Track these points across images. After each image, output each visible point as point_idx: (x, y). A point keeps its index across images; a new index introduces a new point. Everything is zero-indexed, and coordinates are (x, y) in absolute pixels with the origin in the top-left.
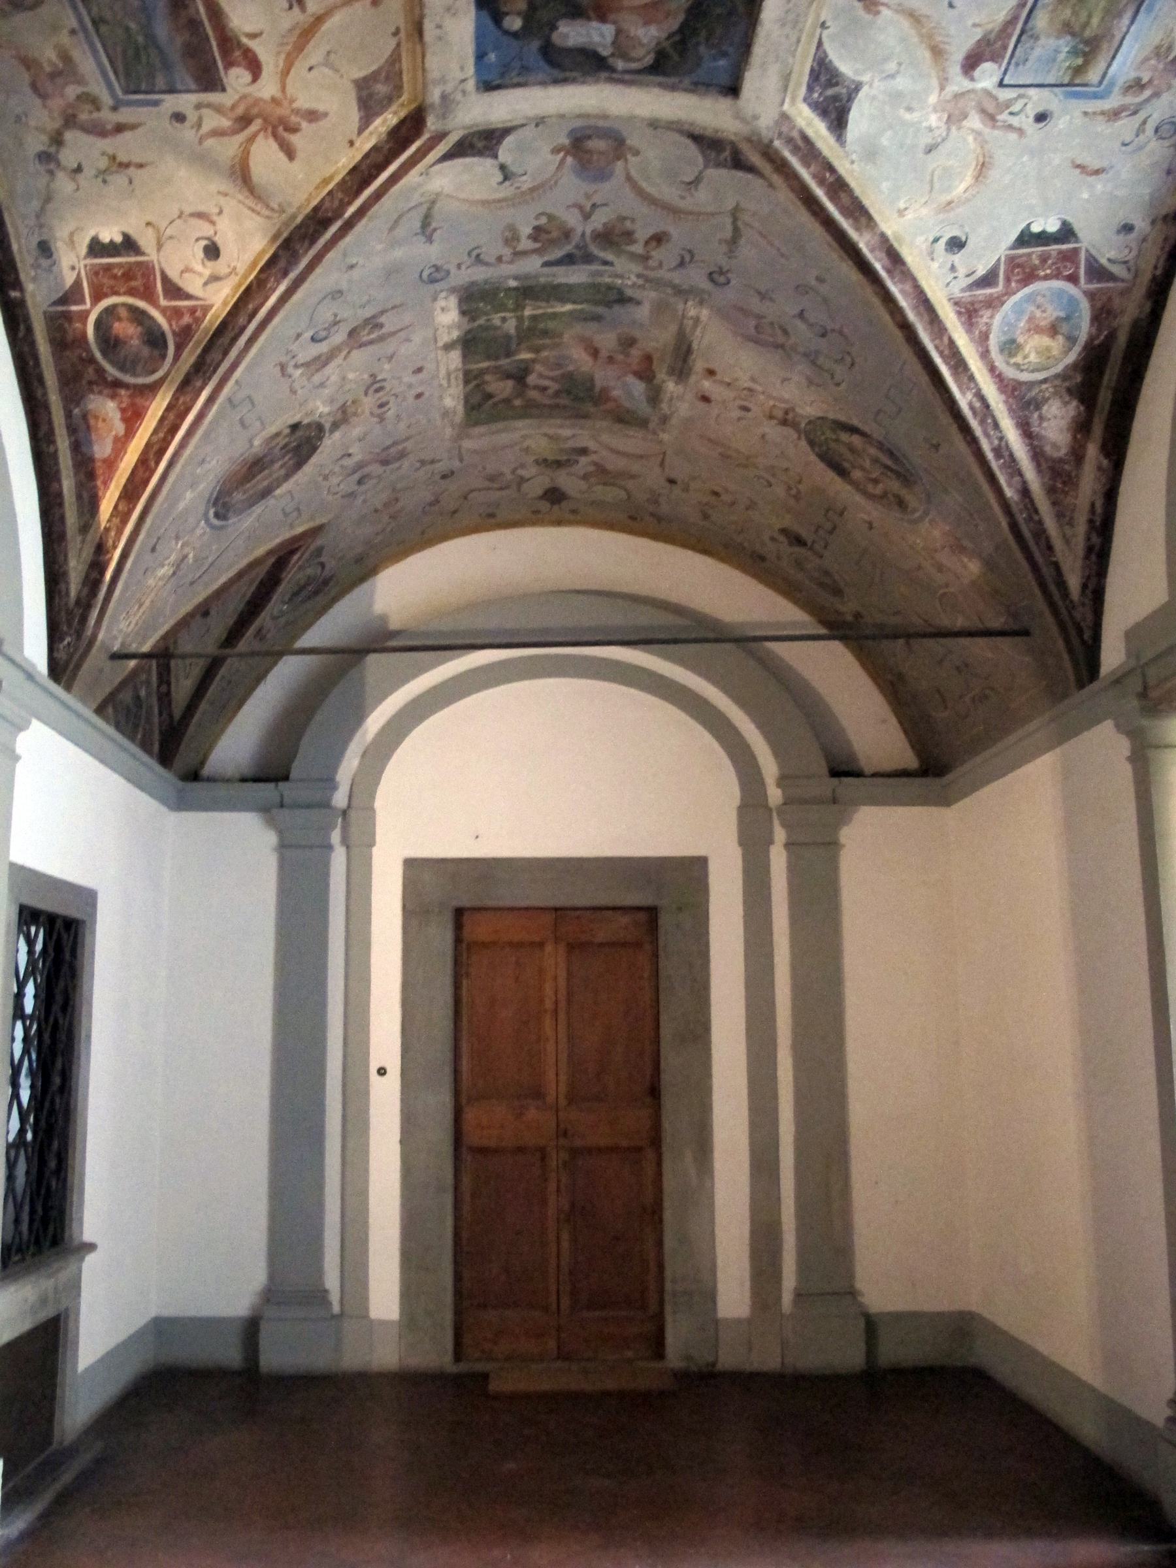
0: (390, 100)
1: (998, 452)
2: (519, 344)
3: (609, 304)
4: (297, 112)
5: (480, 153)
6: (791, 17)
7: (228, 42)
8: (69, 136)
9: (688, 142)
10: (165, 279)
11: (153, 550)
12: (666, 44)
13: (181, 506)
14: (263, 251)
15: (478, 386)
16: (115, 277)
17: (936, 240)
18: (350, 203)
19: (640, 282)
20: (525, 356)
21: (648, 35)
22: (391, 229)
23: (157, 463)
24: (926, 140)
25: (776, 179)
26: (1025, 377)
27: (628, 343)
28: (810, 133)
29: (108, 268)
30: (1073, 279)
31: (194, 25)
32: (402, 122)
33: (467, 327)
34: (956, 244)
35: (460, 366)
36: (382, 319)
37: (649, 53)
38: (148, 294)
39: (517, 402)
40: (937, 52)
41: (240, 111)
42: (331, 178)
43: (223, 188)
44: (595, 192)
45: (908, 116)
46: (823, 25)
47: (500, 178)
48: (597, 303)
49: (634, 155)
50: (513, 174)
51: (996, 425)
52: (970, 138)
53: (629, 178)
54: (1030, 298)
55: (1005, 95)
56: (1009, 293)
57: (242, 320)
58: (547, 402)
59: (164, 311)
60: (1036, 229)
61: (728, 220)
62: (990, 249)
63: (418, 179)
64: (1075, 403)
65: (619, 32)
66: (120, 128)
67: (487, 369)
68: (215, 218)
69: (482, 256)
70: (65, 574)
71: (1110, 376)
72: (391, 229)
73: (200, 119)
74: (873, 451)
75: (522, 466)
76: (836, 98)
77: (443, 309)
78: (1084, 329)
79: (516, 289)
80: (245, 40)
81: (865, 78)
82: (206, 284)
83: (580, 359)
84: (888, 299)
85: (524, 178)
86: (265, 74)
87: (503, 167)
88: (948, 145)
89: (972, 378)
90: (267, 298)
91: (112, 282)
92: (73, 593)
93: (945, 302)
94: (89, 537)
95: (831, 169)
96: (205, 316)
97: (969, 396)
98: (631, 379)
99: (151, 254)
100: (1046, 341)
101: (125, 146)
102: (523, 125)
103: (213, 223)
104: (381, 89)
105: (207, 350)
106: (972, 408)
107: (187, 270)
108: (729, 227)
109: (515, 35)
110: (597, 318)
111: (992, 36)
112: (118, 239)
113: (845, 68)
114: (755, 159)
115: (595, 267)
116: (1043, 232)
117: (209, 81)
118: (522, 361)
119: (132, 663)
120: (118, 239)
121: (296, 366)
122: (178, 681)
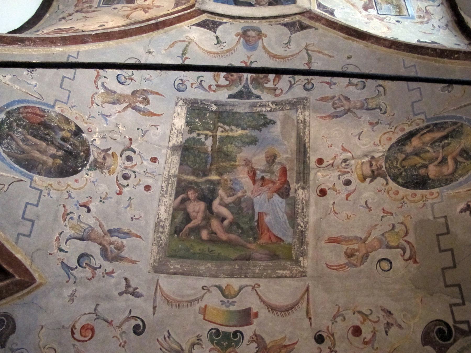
2: (211, 164)
3: (258, 128)
5: (210, 29)
9: (283, 27)
19: (274, 107)
20: (214, 177)
22: (171, 46)
25: (317, 24)
27: (272, 159)
33: (187, 136)
35: (177, 173)
36: (150, 97)
37: (266, 3)
44: (251, 55)
47: (216, 43)
48: (255, 128)
49: (265, 37)
50: (221, 42)
53: (264, 47)
61: (304, 52)
63: (186, 27)
67: (190, 182)
69: (203, 83)
72: (171, 46)
74: (428, 138)
77: (178, 114)
81: (335, 8)
85: (224, 44)
87: (217, 38)
98: (276, 198)
102: (226, 23)
108: (306, 56)
110: (254, 141)
118: (211, 182)
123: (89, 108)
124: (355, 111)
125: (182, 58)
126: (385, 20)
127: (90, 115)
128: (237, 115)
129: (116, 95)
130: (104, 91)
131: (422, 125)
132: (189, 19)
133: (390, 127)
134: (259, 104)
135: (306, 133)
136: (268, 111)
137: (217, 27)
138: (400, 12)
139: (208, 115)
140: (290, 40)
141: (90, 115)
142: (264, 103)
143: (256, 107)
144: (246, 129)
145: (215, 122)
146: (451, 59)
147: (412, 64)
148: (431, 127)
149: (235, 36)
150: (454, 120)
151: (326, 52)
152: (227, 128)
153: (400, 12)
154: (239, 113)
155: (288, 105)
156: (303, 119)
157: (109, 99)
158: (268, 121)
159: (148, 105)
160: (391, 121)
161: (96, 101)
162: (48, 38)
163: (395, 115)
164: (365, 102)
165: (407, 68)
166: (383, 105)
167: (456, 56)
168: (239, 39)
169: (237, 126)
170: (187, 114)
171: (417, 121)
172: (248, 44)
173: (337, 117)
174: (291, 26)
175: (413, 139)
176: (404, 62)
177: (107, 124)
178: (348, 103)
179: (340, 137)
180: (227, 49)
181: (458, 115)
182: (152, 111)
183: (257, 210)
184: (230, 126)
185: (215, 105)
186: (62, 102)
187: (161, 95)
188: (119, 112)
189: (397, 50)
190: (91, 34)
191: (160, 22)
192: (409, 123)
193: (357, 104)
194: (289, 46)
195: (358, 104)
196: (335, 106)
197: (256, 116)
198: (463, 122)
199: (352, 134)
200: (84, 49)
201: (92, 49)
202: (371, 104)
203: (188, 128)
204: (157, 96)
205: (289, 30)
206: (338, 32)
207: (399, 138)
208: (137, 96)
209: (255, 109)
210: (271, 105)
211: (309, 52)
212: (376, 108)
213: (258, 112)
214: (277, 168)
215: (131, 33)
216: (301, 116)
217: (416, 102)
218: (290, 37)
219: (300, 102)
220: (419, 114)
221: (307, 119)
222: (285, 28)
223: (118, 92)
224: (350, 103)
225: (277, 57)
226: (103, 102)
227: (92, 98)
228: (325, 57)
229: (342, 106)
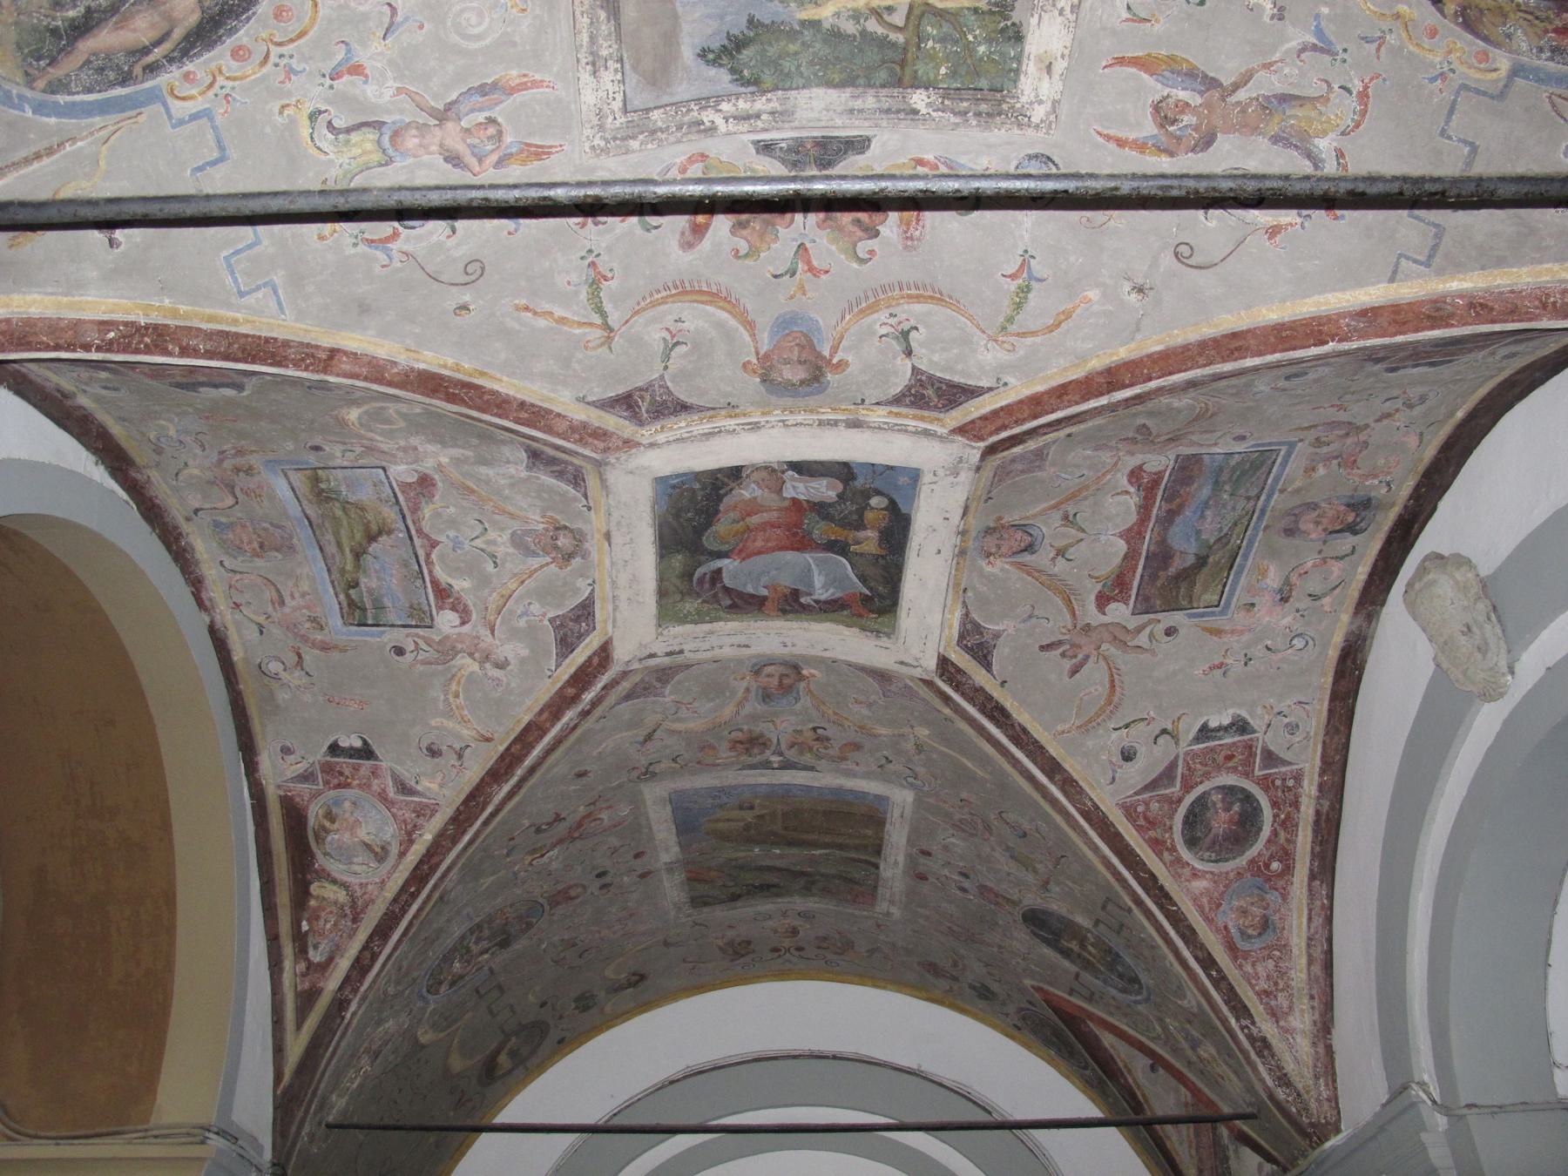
6: (624, 529)
19: (708, 116)
21: (747, 492)
22: (1068, 315)
25: (580, 414)
36: (1149, 129)
46: (589, 509)
47: (913, 334)
53: (750, 325)
61: (614, 319)
72: (1068, 315)
77: (1049, 68)
79: (915, 85)
85: (884, 330)
87: (909, 353)
104: (1019, 467)
109: (878, 493)
114: (612, 422)
115: (783, 135)
123: (1378, 76)
124: (422, 118)
125: (1031, 277)
126: (358, 450)
127: (1378, 50)
128: (837, 78)
129: (1274, 128)
130: (1316, 141)
131: (170, 77)
132: (1002, 409)
133: (285, 61)
134: (759, 123)
135: (586, 20)
136: (728, 97)
137: (909, 388)
138: (316, 480)
139: (943, 71)
140: (666, 357)
141: (1378, 50)
142: (744, 126)
143: (772, 113)
144: (803, 23)
145: (919, 48)
146: (126, 324)
147: (250, 300)
148: (138, 70)
149: (850, 359)
150: (62, 99)
151: (542, 323)
152: (872, 26)
153: (316, 480)
154: (830, 84)
155: (660, 124)
156: (602, 72)
157: (1300, 113)
158: (725, 60)
159: (1157, 98)
160: (288, 85)
161: (1352, 103)
162: (1493, 322)
163: (276, 110)
164: (391, 152)
165: (265, 285)
166: (324, 145)
167: (112, 335)
168: (835, 349)
169: (836, 35)
170: (1017, 71)
171: (194, 92)
172: (806, 336)
173: (483, 90)
175: (194, 19)
176: (280, 303)
177: (1317, 17)
178: (449, 142)
179: (462, 11)
180: (876, 316)
181: (53, 120)
182: (1145, 76)
184: (864, 33)
185: (915, 112)
186: (1478, 91)
187: (1108, 138)
188: (1266, 66)
189: (308, 345)
190: (1340, 341)
191: (1102, 394)
192: (221, 81)
193: (416, 141)
194: (668, 337)
195: (411, 142)
196: (492, 131)
197: (768, 79)
198: (29, 93)
199: (421, 27)
200: (1372, 290)
201: (1343, 290)
202: (369, 146)
203: (1015, 19)
204: (1121, 135)
205: (670, 393)
206: (511, 393)
207: (249, 19)
208: (1196, 129)
209: (775, 105)
210: (719, 121)
211: (599, 321)
212: (348, 130)
213: (764, 92)
215: (1200, 355)
216: (609, 86)
217: (214, 163)
218: (666, 368)
219: (615, 139)
220: (194, 117)
221: (586, 76)
222: (682, 397)
223: (1263, 142)
224: (441, 146)
225: (704, 298)
226: (1324, 99)
227: (1364, 113)
228: (547, 307)
229: (467, 130)
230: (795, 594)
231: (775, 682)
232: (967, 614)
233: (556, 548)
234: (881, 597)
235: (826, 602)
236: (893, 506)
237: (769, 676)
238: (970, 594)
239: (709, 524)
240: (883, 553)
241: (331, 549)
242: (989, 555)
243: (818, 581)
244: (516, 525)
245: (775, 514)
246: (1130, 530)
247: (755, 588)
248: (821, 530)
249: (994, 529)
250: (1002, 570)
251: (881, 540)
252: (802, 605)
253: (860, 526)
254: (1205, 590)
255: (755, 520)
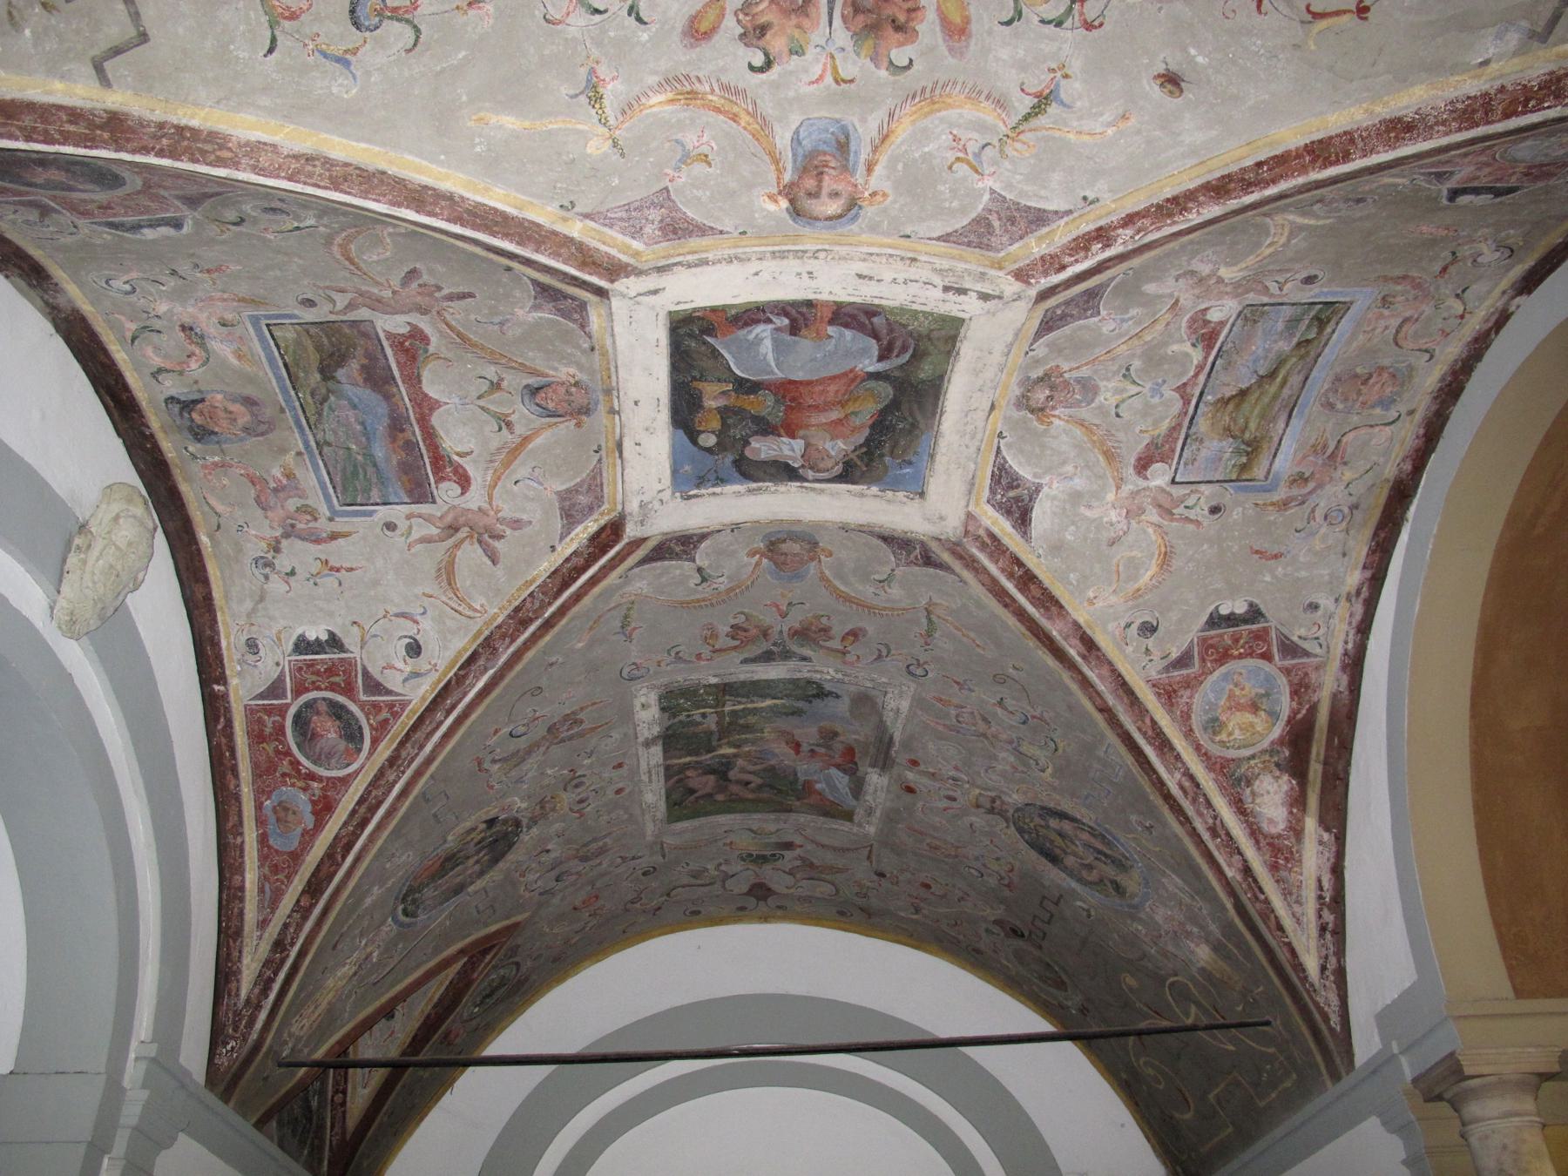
0: (591, 509)
1: (1214, 832)
3: (808, 699)
4: (501, 521)
5: (678, 557)
6: (970, 428)
7: (439, 460)
8: (284, 543)
9: (879, 542)
10: (366, 673)
11: (334, 947)
12: (853, 456)
13: (368, 901)
14: (465, 649)
15: (680, 780)
16: (318, 673)
17: (1128, 625)
18: (550, 604)
21: (837, 448)
23: (344, 858)
24: (1106, 535)
25: (967, 575)
26: (1232, 754)
27: (829, 736)
28: (996, 530)
29: (311, 664)
30: (1267, 656)
31: (410, 446)
32: (602, 529)
34: (1148, 629)
35: (661, 761)
36: (581, 716)
38: (349, 690)
39: (720, 797)
40: (1110, 456)
41: (449, 519)
42: (533, 580)
43: (428, 591)
45: (1088, 513)
46: (1000, 436)
47: (698, 580)
51: (1209, 804)
52: (1150, 530)
53: (823, 578)
54: (1225, 677)
55: (1178, 491)
56: (1205, 673)
57: (439, 716)
58: (750, 796)
59: (362, 706)
60: (1224, 611)
62: (1183, 633)
64: (1286, 777)
65: (807, 445)
66: (334, 536)
68: (418, 618)
70: (239, 971)
71: (1318, 749)
73: (410, 527)
74: (1085, 836)
75: (727, 862)
76: (1017, 499)
78: (1285, 705)
80: (456, 458)
82: (405, 680)
83: (782, 754)
84: (1085, 683)
86: (473, 488)
87: (699, 570)
88: (1131, 538)
89: (1178, 757)
90: (465, 694)
91: (314, 678)
92: (243, 993)
93: (1143, 684)
94: (266, 935)
95: (1020, 564)
96: (403, 710)
97: (1178, 776)
98: (833, 771)
99: (354, 651)
100: (1248, 717)
101: (339, 552)
103: (417, 622)
104: (583, 499)
105: (402, 744)
106: (1182, 788)
107: (390, 667)
108: (924, 621)
109: (709, 450)
111: (1160, 441)
112: (324, 637)
113: (1025, 472)
114: (946, 557)
115: (792, 664)
116: (1232, 614)
117: (419, 493)
118: (723, 756)
119: (304, 1070)
120: (324, 637)
121: (494, 761)
122: (354, 1088)
138: (1244, 468)
153: (1244, 468)
174: (901, 548)
183: (802, 778)
214: (838, 746)
230: (794, 330)
231: (828, 184)
232: (583, 327)
233: (1052, 388)
234: (691, 336)
235: (757, 322)
236: (693, 436)
237: (835, 195)
238: (586, 346)
239: (883, 413)
240: (695, 384)
241: (1295, 380)
242: (576, 384)
243: (767, 347)
244: (1084, 413)
245: (813, 421)
246: (432, 409)
247: (842, 335)
248: (765, 404)
249: (580, 412)
250: (556, 369)
251: (700, 398)
252: (787, 315)
253: (724, 412)
254: (298, 343)
255: (835, 415)
